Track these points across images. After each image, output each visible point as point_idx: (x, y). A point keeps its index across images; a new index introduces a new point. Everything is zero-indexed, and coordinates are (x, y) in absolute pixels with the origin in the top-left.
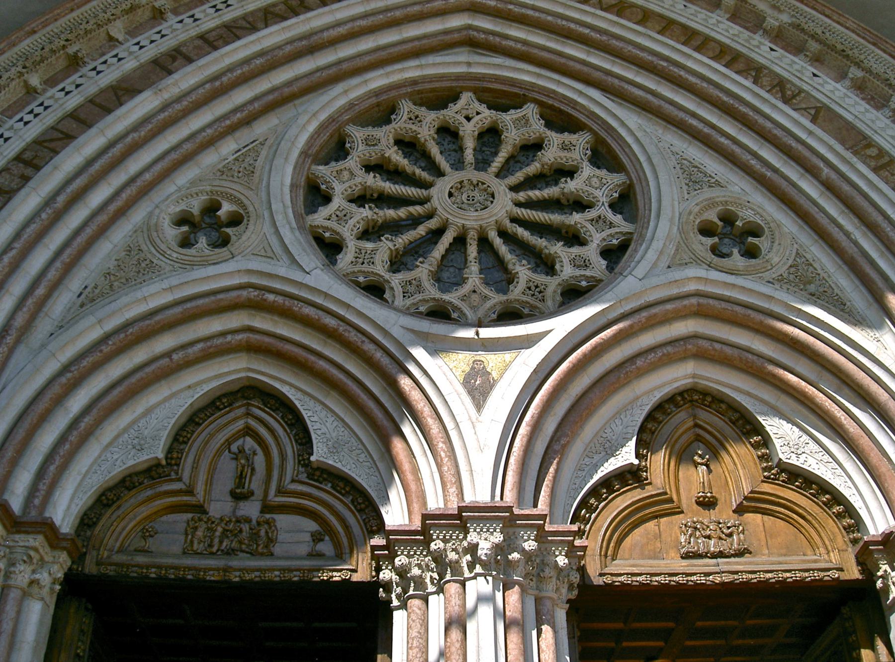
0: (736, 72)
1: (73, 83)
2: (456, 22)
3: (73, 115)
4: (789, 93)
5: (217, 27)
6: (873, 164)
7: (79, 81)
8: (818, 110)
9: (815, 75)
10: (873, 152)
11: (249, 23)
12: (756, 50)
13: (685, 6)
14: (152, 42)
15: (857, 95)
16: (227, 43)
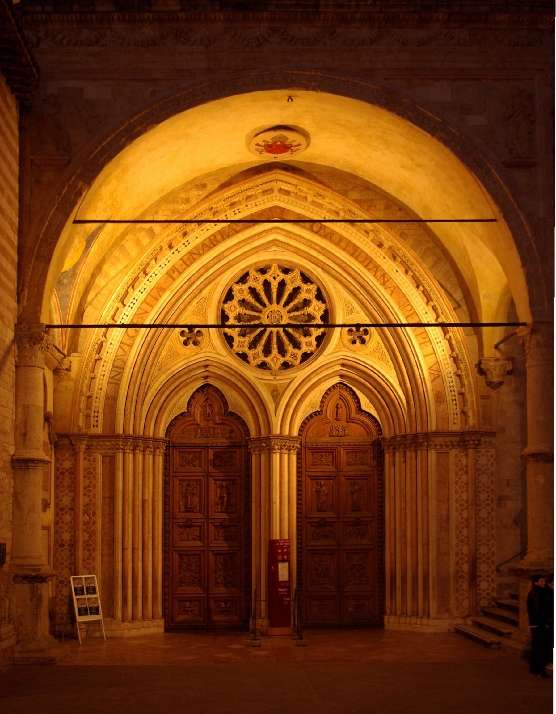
0: (368, 270)
1: (142, 287)
2: (270, 238)
3: (145, 301)
4: (386, 279)
5: (187, 254)
6: (407, 314)
7: (145, 287)
8: (394, 288)
9: (397, 271)
10: (409, 308)
11: (197, 250)
12: (378, 258)
13: (356, 234)
14: (165, 265)
15: (410, 281)
16: (192, 263)
